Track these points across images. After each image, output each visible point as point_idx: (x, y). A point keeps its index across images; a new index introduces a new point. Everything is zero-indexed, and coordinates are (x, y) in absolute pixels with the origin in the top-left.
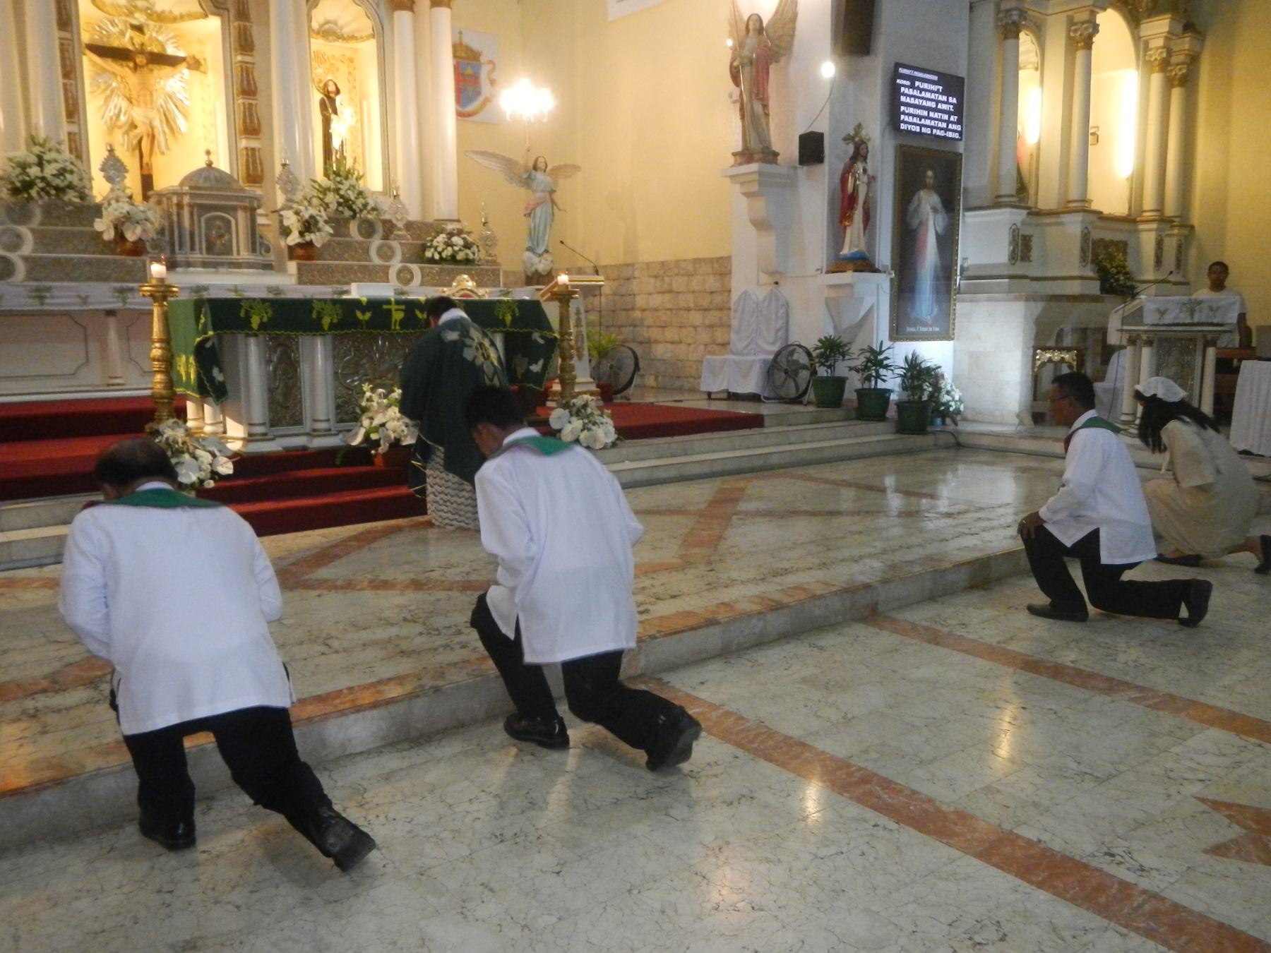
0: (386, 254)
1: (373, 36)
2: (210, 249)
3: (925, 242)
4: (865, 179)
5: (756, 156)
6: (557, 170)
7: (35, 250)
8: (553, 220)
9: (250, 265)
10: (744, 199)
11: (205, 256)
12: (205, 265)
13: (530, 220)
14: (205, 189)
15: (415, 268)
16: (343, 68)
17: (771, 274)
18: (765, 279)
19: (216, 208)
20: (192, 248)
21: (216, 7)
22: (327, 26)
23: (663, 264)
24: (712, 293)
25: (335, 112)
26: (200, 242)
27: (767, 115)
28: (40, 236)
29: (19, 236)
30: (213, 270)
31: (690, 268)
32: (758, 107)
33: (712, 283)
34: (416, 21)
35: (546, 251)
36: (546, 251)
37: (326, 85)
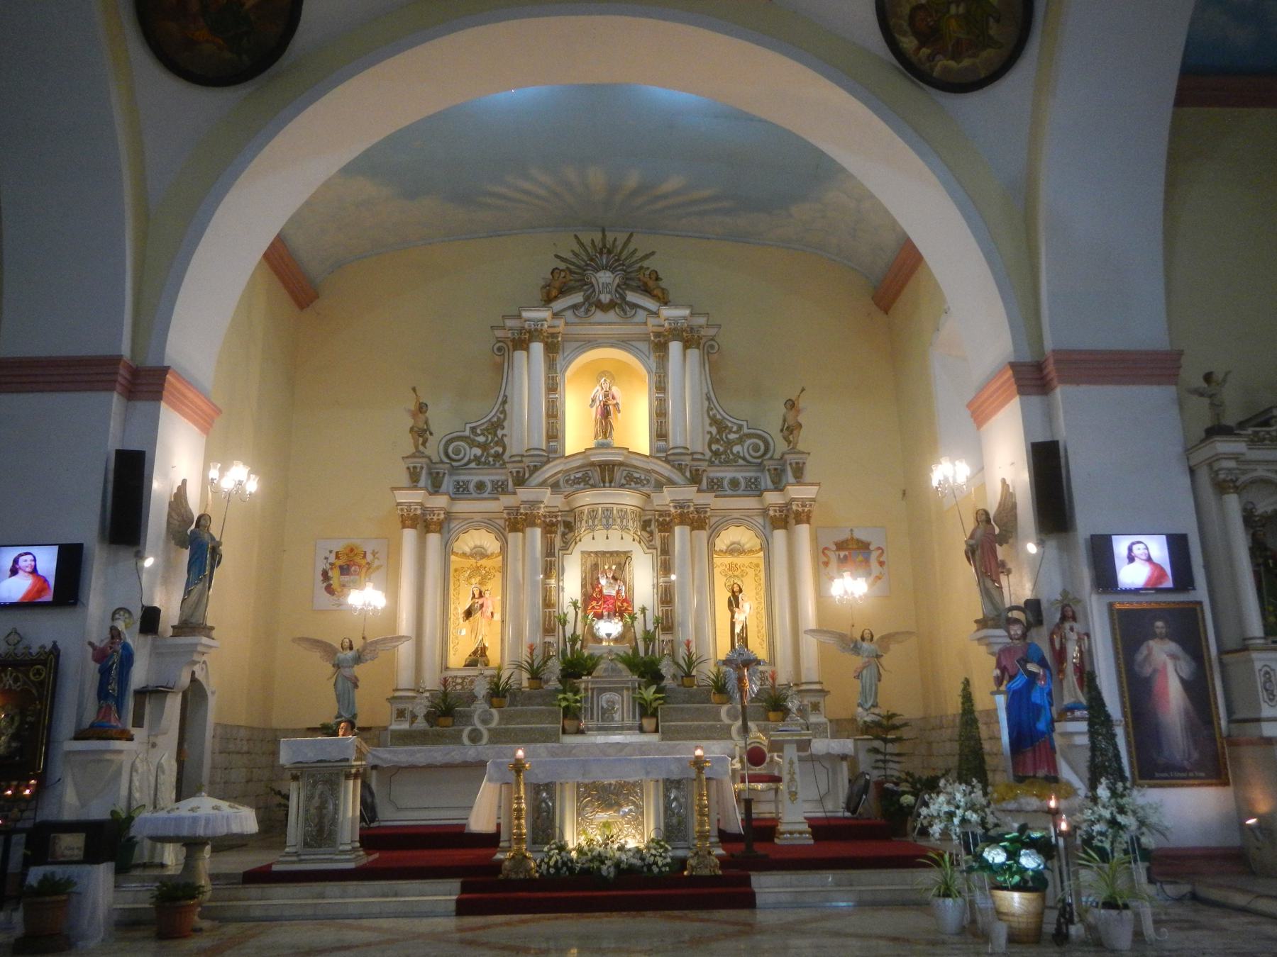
1: (761, 549)
3: (1166, 688)
4: (1074, 636)
5: (990, 623)
6: (887, 639)
7: (500, 723)
8: (879, 680)
9: (630, 728)
12: (600, 729)
13: (859, 681)
14: (606, 677)
16: (751, 572)
20: (592, 718)
21: (648, 548)
22: (732, 547)
25: (737, 606)
26: (598, 714)
28: (501, 713)
29: (491, 715)
32: (989, 583)
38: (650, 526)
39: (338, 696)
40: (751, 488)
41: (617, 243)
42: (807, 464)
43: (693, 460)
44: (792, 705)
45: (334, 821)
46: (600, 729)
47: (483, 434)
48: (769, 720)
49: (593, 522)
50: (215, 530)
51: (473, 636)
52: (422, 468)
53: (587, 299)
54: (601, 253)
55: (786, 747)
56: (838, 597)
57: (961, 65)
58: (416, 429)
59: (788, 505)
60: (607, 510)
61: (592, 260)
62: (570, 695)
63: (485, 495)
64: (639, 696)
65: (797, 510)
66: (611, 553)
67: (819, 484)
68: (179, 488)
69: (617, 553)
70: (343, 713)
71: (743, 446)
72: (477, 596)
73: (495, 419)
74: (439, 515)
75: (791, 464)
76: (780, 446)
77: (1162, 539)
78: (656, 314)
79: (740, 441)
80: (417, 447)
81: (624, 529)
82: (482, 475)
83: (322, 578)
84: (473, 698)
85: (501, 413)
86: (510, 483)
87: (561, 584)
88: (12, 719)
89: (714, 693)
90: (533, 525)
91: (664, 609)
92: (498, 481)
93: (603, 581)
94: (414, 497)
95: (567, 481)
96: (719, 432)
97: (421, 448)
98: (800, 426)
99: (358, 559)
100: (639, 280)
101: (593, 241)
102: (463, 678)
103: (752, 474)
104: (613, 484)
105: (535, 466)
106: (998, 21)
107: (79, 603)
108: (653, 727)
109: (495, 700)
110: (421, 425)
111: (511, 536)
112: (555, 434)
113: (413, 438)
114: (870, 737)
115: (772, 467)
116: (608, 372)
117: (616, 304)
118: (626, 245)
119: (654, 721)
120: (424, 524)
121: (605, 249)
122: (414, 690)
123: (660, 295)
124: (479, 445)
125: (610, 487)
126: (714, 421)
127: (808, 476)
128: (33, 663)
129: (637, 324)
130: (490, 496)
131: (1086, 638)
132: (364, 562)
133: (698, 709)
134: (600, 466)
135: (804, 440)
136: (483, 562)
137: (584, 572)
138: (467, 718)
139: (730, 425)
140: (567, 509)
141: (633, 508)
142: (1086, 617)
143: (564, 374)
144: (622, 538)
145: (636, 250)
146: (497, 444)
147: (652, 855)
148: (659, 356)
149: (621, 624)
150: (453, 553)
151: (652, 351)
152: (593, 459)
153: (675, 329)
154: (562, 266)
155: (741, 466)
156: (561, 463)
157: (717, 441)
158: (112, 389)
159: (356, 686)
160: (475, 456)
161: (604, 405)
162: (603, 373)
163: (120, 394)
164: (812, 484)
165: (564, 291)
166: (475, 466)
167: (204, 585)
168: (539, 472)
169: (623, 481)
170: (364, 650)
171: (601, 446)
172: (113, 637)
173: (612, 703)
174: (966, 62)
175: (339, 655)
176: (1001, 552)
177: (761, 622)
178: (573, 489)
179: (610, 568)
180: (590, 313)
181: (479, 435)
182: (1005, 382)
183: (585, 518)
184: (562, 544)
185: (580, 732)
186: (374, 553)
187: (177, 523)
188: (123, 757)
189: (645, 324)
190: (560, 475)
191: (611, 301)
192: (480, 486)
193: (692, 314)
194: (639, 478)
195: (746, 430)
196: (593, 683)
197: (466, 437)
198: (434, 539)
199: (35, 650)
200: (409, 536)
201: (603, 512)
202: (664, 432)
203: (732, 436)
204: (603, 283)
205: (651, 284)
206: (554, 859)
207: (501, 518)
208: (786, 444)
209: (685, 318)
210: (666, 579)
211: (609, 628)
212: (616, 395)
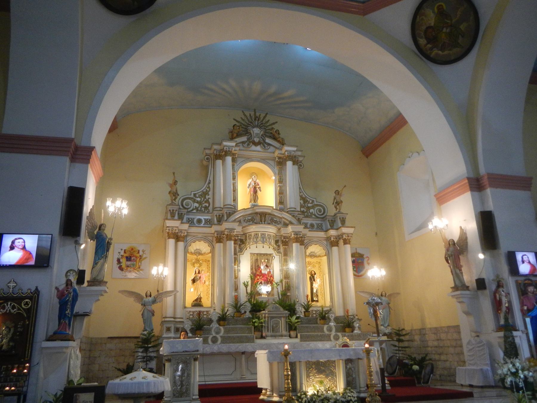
0: (330, 330)
1: (326, 255)
2: (273, 331)
5: (460, 288)
6: (390, 295)
8: (390, 314)
9: (285, 336)
10: (459, 304)
11: (272, 333)
12: (272, 336)
14: (273, 311)
15: (339, 334)
16: (317, 266)
17: (476, 332)
18: (474, 334)
19: (276, 317)
20: (268, 331)
21: (278, 253)
22: (311, 254)
23: (436, 328)
24: (456, 340)
25: (314, 280)
26: (270, 329)
27: (462, 273)
28: (225, 329)
29: (220, 329)
31: (446, 330)
32: (458, 271)
33: (455, 336)
34: (339, 250)
35: (388, 326)
36: (388, 326)
37: (311, 272)
38: (278, 243)
39: (144, 320)
40: (319, 228)
41: (261, 116)
42: (346, 219)
43: (299, 214)
44: (356, 325)
45: (189, 384)
46: (274, 336)
47: (199, 197)
48: (345, 332)
49: (257, 240)
50: (108, 232)
51: (196, 292)
52: (176, 210)
53: (248, 139)
54: (255, 120)
55: (375, 343)
56: (371, 277)
57: (444, 53)
58: (172, 192)
59: (339, 237)
60: (263, 234)
61: (251, 122)
62: (257, 320)
63: (202, 225)
64: (289, 320)
65: (345, 238)
66: (264, 254)
67: (354, 227)
68: (91, 209)
69: (267, 254)
71: (314, 210)
72: (197, 272)
73: (205, 191)
74: (184, 233)
75: (340, 218)
76: (331, 211)
77: (533, 254)
78: (281, 150)
79: (313, 207)
80: (172, 201)
81: (270, 244)
82: (200, 216)
83: (117, 262)
84: (210, 321)
85: (208, 188)
86: (215, 219)
87: (239, 268)
88: (10, 330)
89: (320, 320)
90: (231, 240)
91: (286, 281)
92: (208, 219)
93: (262, 267)
94: (173, 224)
95: (244, 221)
96: (304, 202)
97: (174, 201)
98: (342, 202)
99: (136, 254)
100: (271, 133)
101: (250, 114)
102: (193, 312)
103: (319, 222)
104: (266, 223)
105: (230, 213)
106: (463, 37)
107: (49, 266)
108: (295, 336)
109: (222, 322)
110: (175, 191)
111: (218, 245)
112: (235, 200)
113: (170, 195)
114: (390, 339)
115: (330, 219)
116: (255, 173)
117: (261, 143)
118: (265, 117)
119: (295, 332)
120: (176, 237)
121: (257, 118)
122: (172, 317)
123: (281, 141)
124: (197, 202)
125: (265, 224)
126: (302, 198)
127: (347, 224)
128: (23, 298)
129: (271, 152)
130: (204, 225)
131: (508, 295)
132: (138, 255)
133: (314, 327)
134: (260, 214)
135: (344, 208)
136: (200, 257)
137: (252, 263)
138: (209, 331)
139: (309, 200)
140: (242, 234)
141: (273, 234)
142: (507, 285)
143: (237, 172)
144: (263, 247)
145: (269, 120)
146: (206, 202)
147: (349, 396)
148: (280, 167)
149: (271, 287)
150: (188, 252)
151: (276, 166)
152: (257, 211)
153: (290, 156)
154: (238, 124)
155: (313, 218)
156: (243, 212)
157: (303, 207)
158: (67, 156)
159: (153, 315)
160: (195, 207)
161: (255, 187)
162: (252, 173)
163: (69, 158)
164: (352, 227)
165: (239, 135)
166: (195, 212)
167: (104, 261)
168: (233, 215)
169: (269, 222)
170: (157, 297)
171: (254, 206)
172: (67, 285)
173: (277, 324)
174: (446, 52)
175: (145, 299)
176: (461, 257)
177: (322, 288)
178: (247, 224)
179: (265, 261)
180: (249, 146)
181: (197, 197)
182: (464, 184)
183: (252, 237)
184: (239, 250)
185: (262, 337)
186: (143, 251)
187: (90, 228)
188: (68, 351)
189: (274, 153)
190: (241, 218)
191: (259, 141)
192: (199, 221)
193: (297, 150)
194: (277, 221)
195: (315, 203)
196: (268, 314)
197: (193, 198)
198: (181, 244)
199: (25, 290)
200: (172, 242)
201: (261, 235)
202: (282, 201)
203: (309, 205)
204: (256, 133)
205: (277, 136)
206: (304, 400)
207: (211, 236)
208: (335, 209)
209: (294, 151)
210: (287, 267)
211: (265, 289)
212: (259, 184)
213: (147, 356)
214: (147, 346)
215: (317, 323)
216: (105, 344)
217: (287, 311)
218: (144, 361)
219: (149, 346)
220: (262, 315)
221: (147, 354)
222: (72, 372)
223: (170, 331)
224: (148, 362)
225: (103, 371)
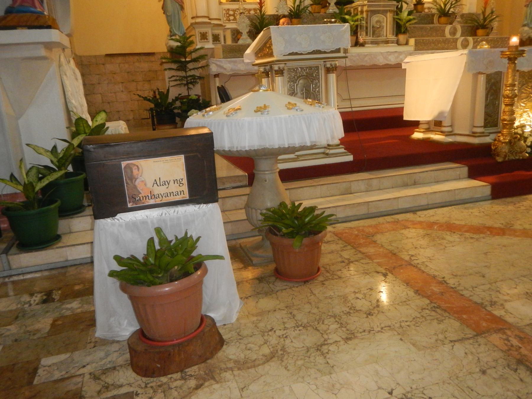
0: (453, 32)
12: (373, 43)
15: (470, 39)
30: (377, 45)
39: (167, 16)
44: (495, 24)
70: (177, 33)
89: (440, 17)
102: (234, 11)
108: (405, 42)
133: (431, 28)
196: (369, 6)
213: (187, 77)
214: (184, 60)
215: (433, 23)
216: (103, 64)
217: (395, 2)
218: (185, 85)
219: (187, 60)
220: (357, 9)
221: (186, 72)
222: (73, 101)
223: (207, 39)
224: (191, 86)
225: (109, 103)
